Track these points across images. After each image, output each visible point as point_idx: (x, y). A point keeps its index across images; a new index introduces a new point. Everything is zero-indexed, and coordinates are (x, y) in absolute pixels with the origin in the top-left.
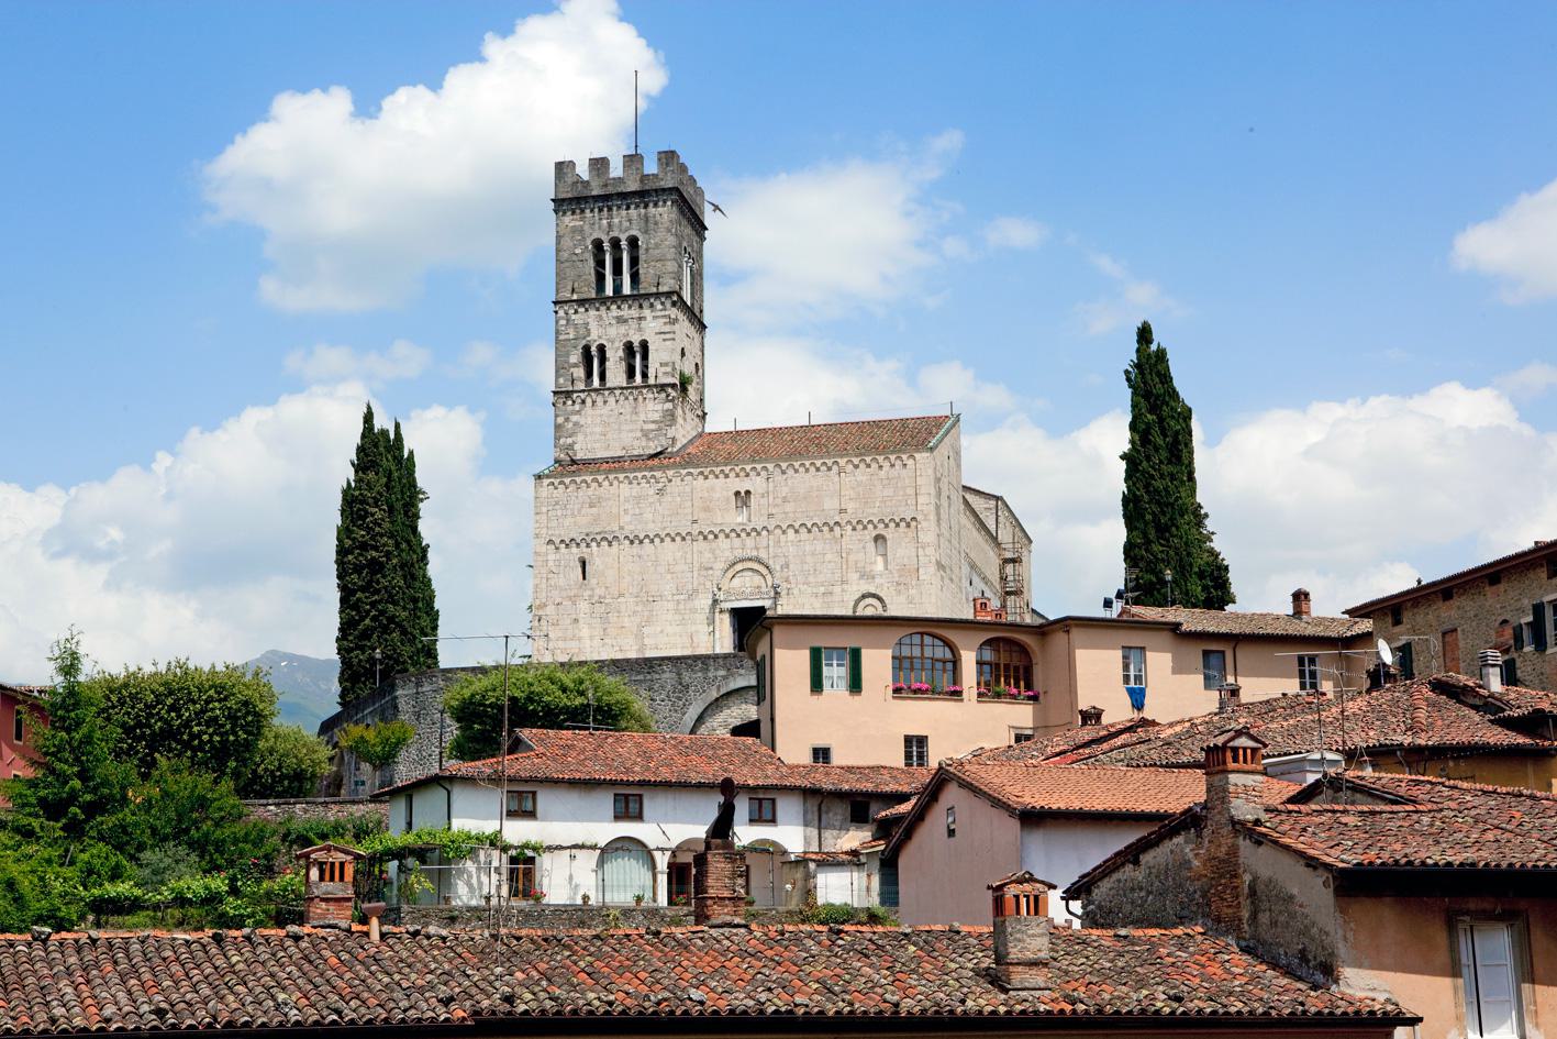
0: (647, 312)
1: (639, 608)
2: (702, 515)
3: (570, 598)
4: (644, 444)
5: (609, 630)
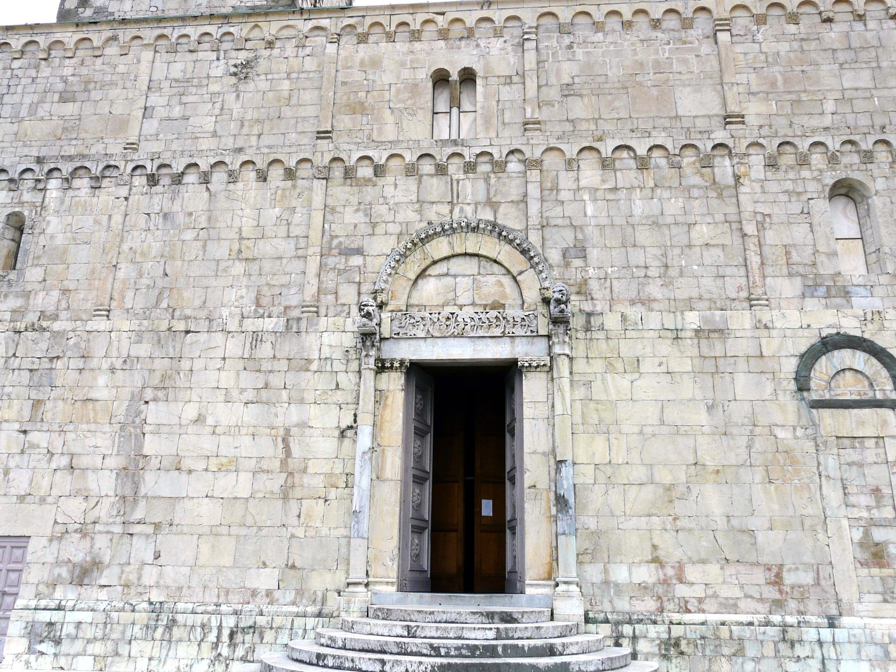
1: (143, 350)
2: (345, 122)
5: (49, 405)
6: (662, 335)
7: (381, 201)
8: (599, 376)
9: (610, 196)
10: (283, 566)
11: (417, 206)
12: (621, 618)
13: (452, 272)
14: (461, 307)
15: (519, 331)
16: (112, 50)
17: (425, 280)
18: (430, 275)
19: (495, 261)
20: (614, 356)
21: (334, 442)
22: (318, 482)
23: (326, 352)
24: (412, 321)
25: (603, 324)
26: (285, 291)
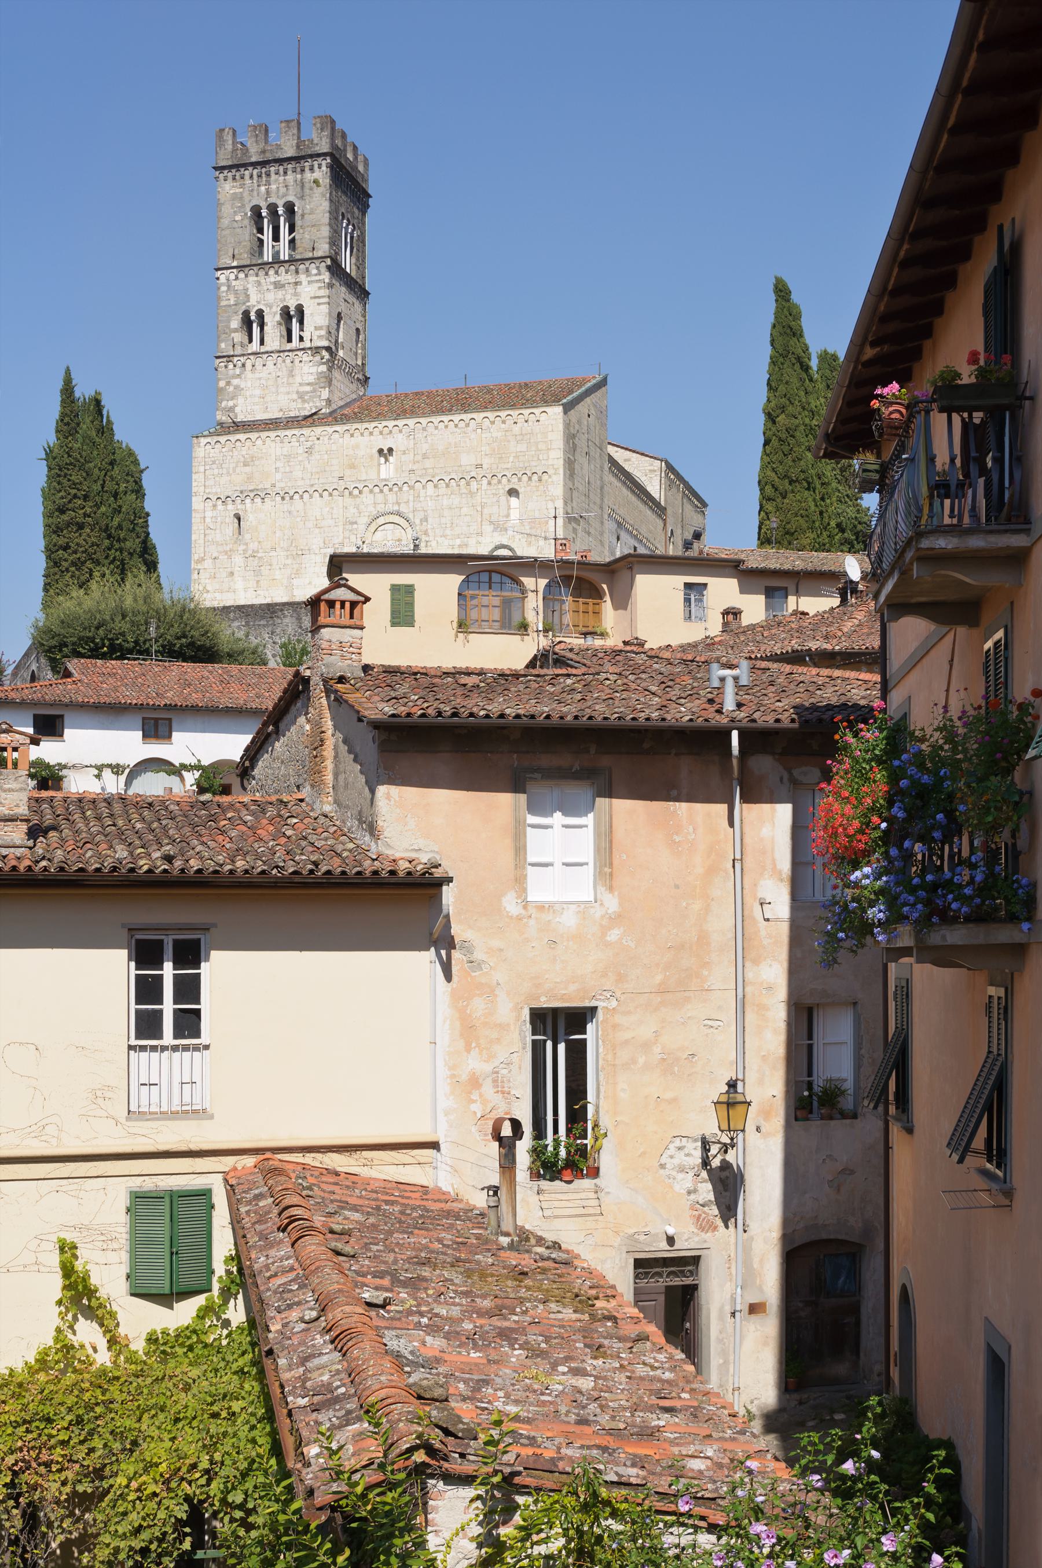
0: (302, 277)
1: (289, 561)
2: (348, 472)
3: (226, 553)
4: (299, 406)
16: (259, 442)
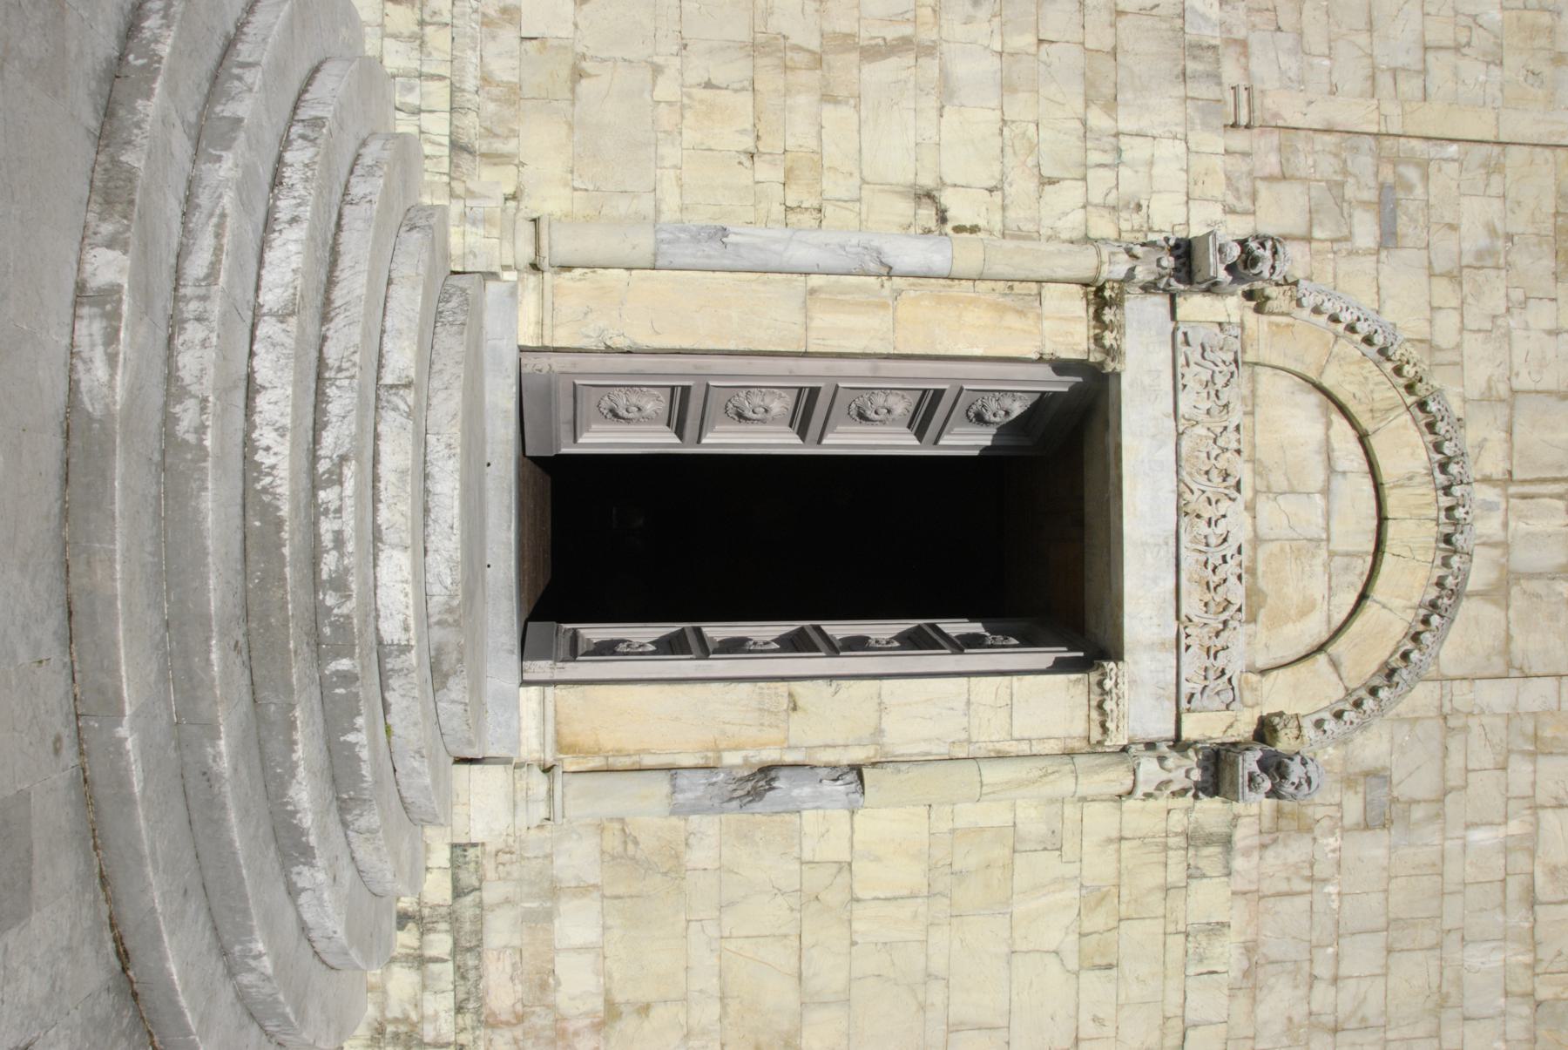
6: (1170, 1023)
7: (1517, 295)
8: (1072, 870)
9: (1515, 887)
10: (580, 49)
11: (1502, 390)
12: (467, 927)
13: (1337, 482)
14: (1251, 508)
15: (1193, 662)
17: (1316, 412)
18: (1329, 425)
19: (1363, 597)
20: (1123, 907)
21: (903, 173)
22: (799, 135)
23: (1135, 150)
24: (1220, 380)
25: (1204, 876)
26: (1287, 40)
